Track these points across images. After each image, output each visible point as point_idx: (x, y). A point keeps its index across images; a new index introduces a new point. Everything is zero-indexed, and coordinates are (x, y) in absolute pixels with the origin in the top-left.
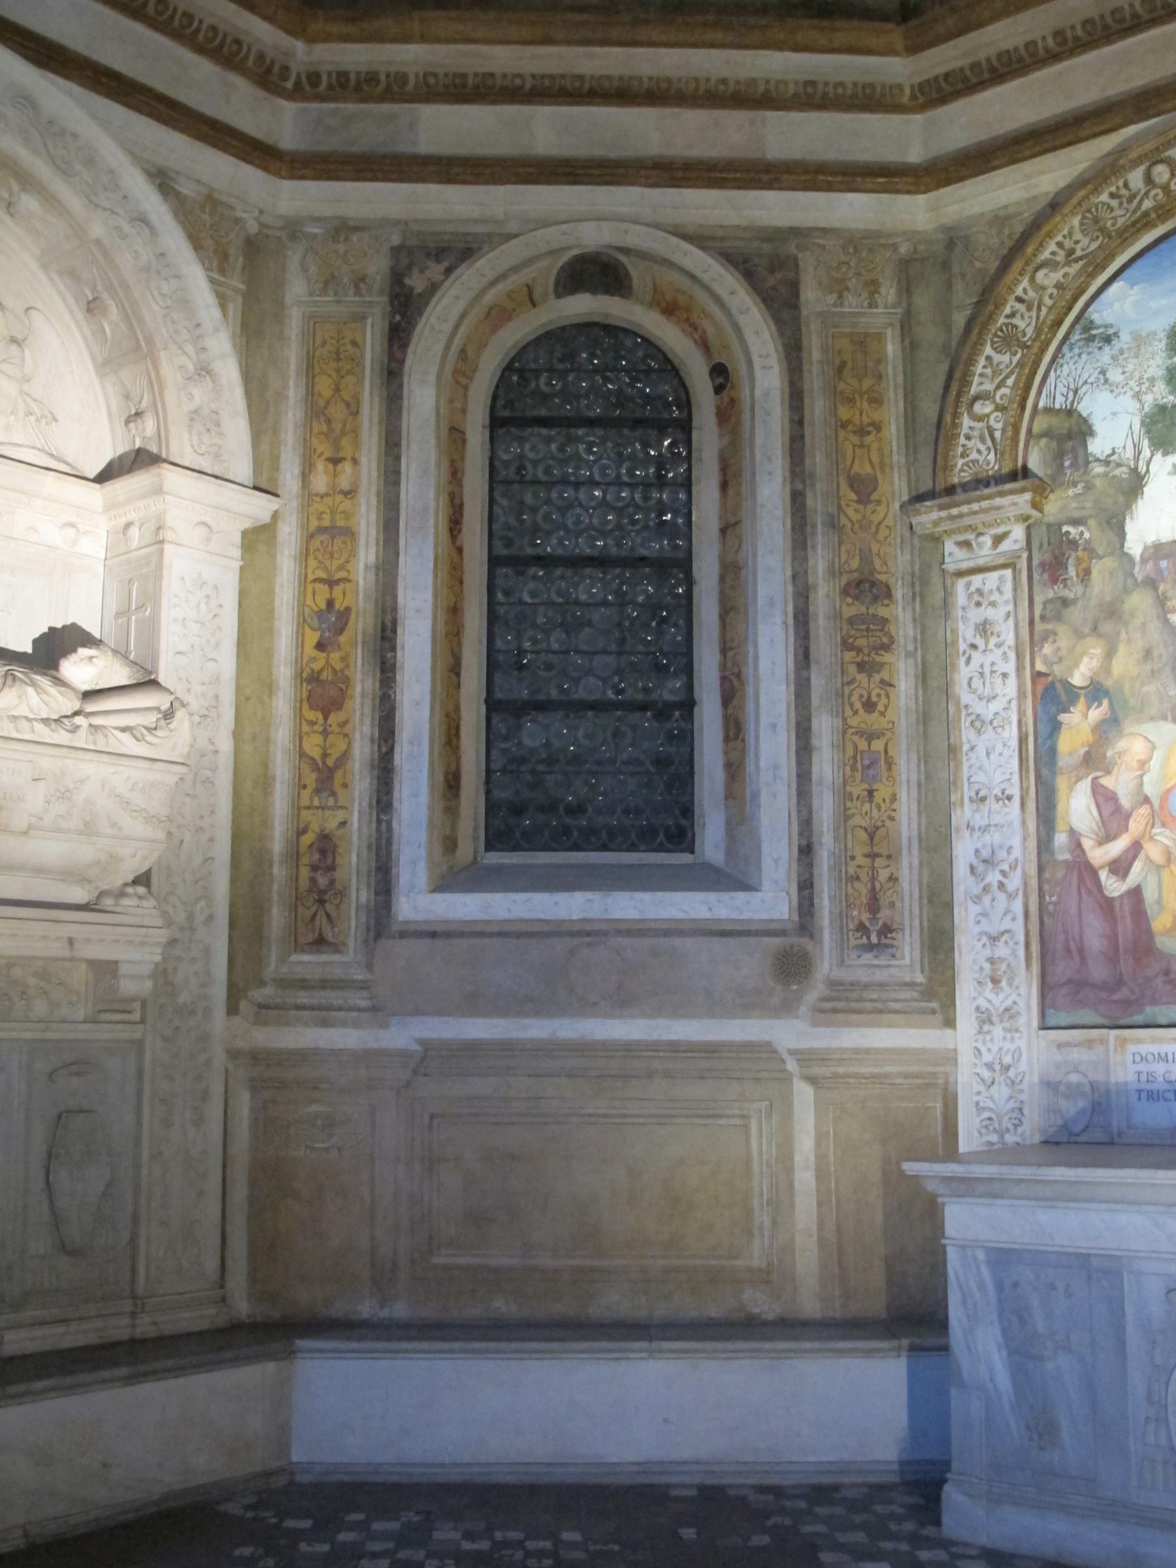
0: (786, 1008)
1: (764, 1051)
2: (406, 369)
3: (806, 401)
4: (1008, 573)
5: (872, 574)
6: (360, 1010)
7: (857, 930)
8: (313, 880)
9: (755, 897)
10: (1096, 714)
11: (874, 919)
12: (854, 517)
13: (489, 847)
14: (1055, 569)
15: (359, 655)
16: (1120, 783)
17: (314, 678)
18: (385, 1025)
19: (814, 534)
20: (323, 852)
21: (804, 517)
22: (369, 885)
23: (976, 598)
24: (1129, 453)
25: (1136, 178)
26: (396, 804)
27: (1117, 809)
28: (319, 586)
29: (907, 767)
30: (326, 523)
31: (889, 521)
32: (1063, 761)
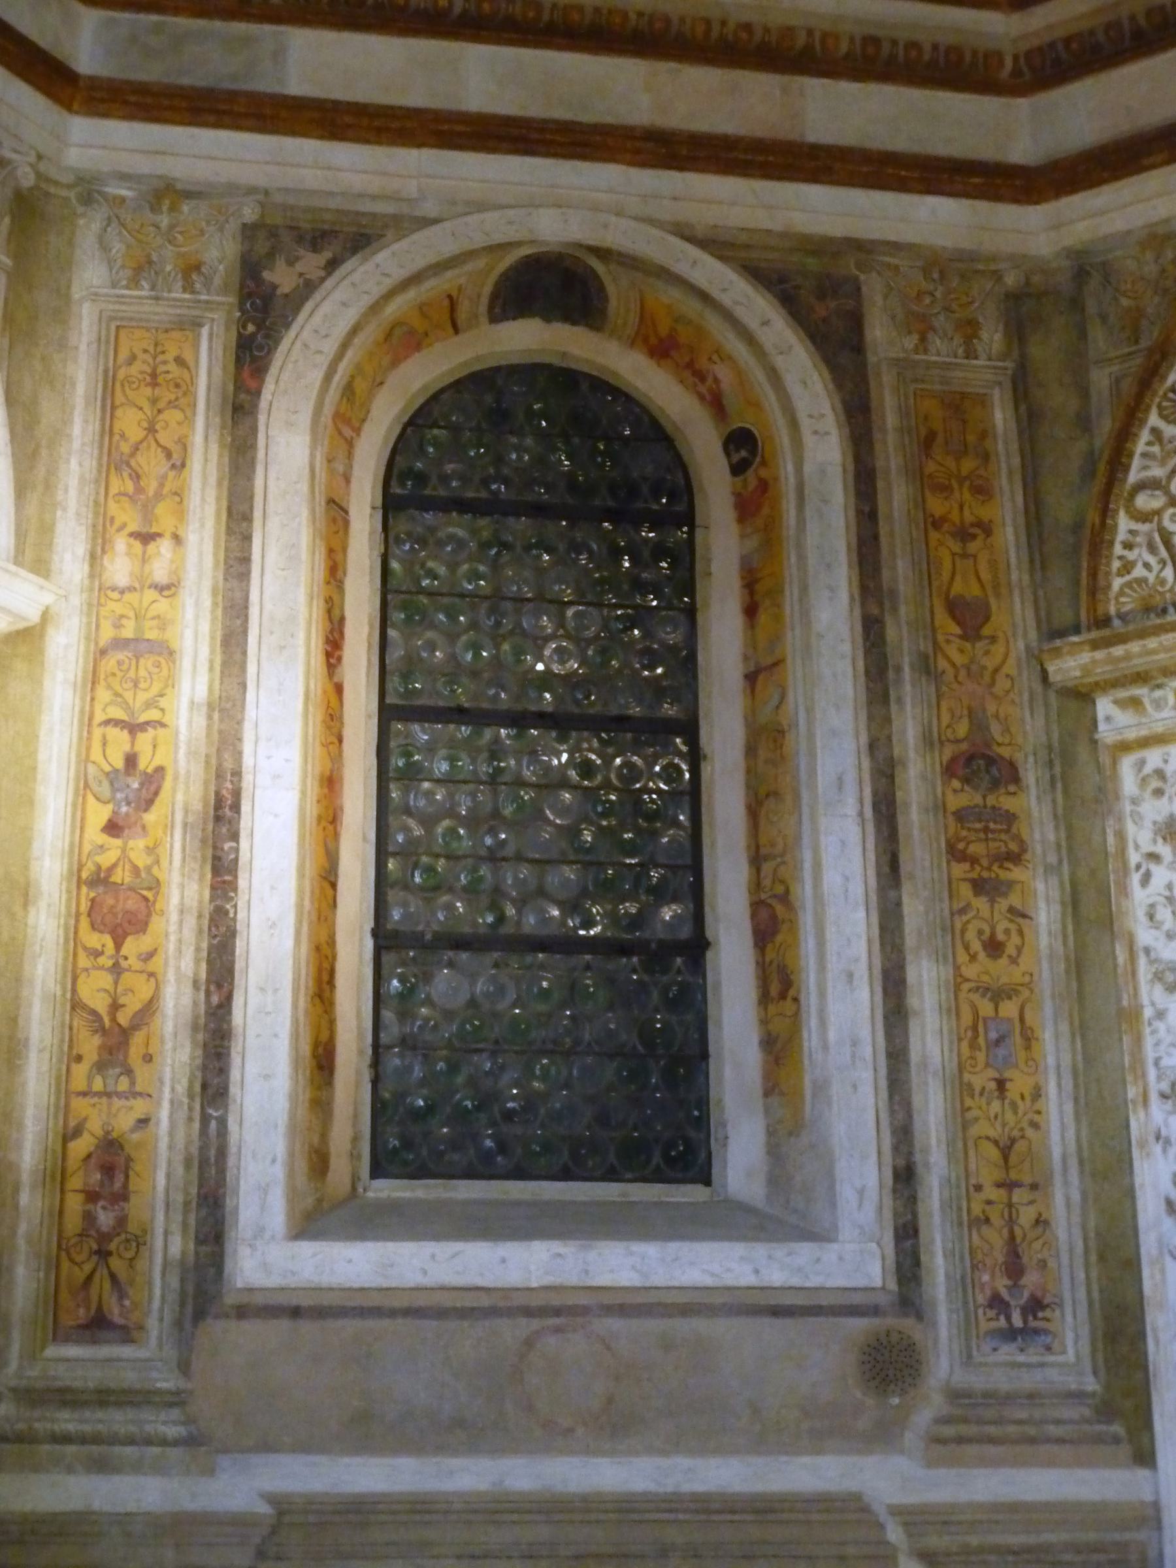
2: (263, 404)
3: (880, 484)
5: (988, 745)
6: (164, 1442)
7: (990, 1306)
8: (89, 1218)
9: (830, 1253)
11: (1015, 1287)
12: (958, 659)
13: (377, 1171)
15: (178, 846)
17: (101, 879)
18: (210, 1471)
19: (899, 681)
20: (108, 1170)
21: (884, 657)
22: (185, 1225)
23: (1155, 783)
26: (234, 1090)
28: (113, 732)
30: (128, 632)
31: (1010, 668)
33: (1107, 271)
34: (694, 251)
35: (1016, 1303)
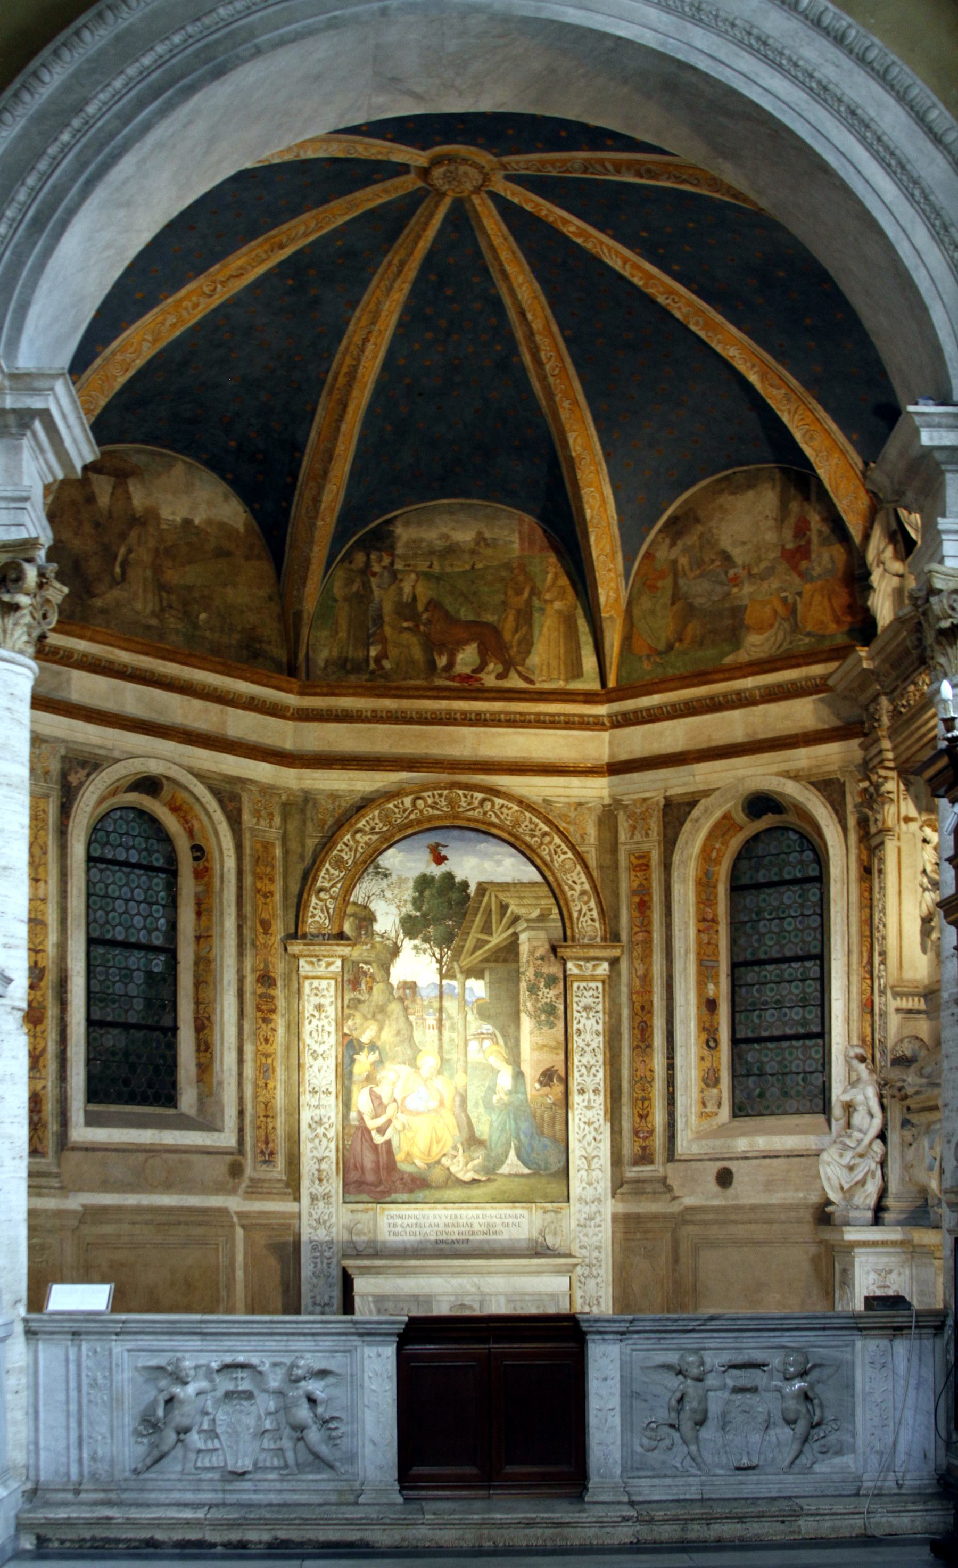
6: (51, 1188)
9: (222, 1135)
10: (374, 1056)
16: (383, 1091)
18: (67, 1197)
24: (393, 935)
25: (408, 801)
27: (381, 1103)
29: (280, 1073)
32: (356, 1077)
33: (315, 804)
34: (195, 781)
35: (267, 1152)
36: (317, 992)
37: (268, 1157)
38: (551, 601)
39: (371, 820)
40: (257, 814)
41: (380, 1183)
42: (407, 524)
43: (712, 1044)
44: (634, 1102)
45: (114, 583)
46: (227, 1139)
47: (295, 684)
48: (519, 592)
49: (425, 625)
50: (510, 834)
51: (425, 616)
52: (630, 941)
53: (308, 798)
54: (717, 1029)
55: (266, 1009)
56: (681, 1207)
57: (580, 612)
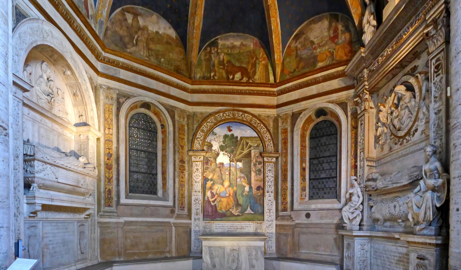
0: (172, 217)
1: (169, 223)
4: (201, 163)
10: (211, 183)
14: (207, 163)
16: (214, 191)
24: (217, 150)
25: (221, 114)
32: (207, 188)
33: (196, 115)
36: (197, 165)
37: (182, 208)
38: (261, 61)
39: (212, 119)
40: (180, 117)
41: (213, 215)
42: (221, 40)
43: (304, 180)
44: (282, 195)
45: (133, 45)
46: (170, 203)
47: (190, 81)
48: (253, 58)
49: (226, 67)
50: (249, 123)
51: (226, 65)
52: (282, 152)
53: (195, 114)
54: (305, 176)
55: (182, 169)
56: (295, 223)
57: (269, 64)
